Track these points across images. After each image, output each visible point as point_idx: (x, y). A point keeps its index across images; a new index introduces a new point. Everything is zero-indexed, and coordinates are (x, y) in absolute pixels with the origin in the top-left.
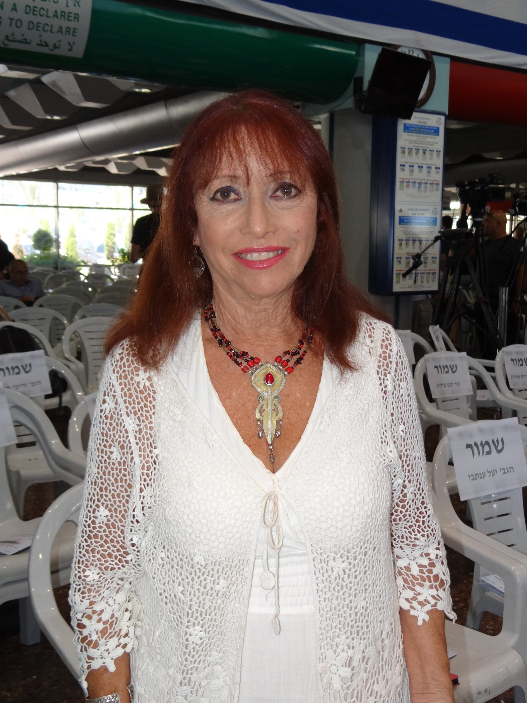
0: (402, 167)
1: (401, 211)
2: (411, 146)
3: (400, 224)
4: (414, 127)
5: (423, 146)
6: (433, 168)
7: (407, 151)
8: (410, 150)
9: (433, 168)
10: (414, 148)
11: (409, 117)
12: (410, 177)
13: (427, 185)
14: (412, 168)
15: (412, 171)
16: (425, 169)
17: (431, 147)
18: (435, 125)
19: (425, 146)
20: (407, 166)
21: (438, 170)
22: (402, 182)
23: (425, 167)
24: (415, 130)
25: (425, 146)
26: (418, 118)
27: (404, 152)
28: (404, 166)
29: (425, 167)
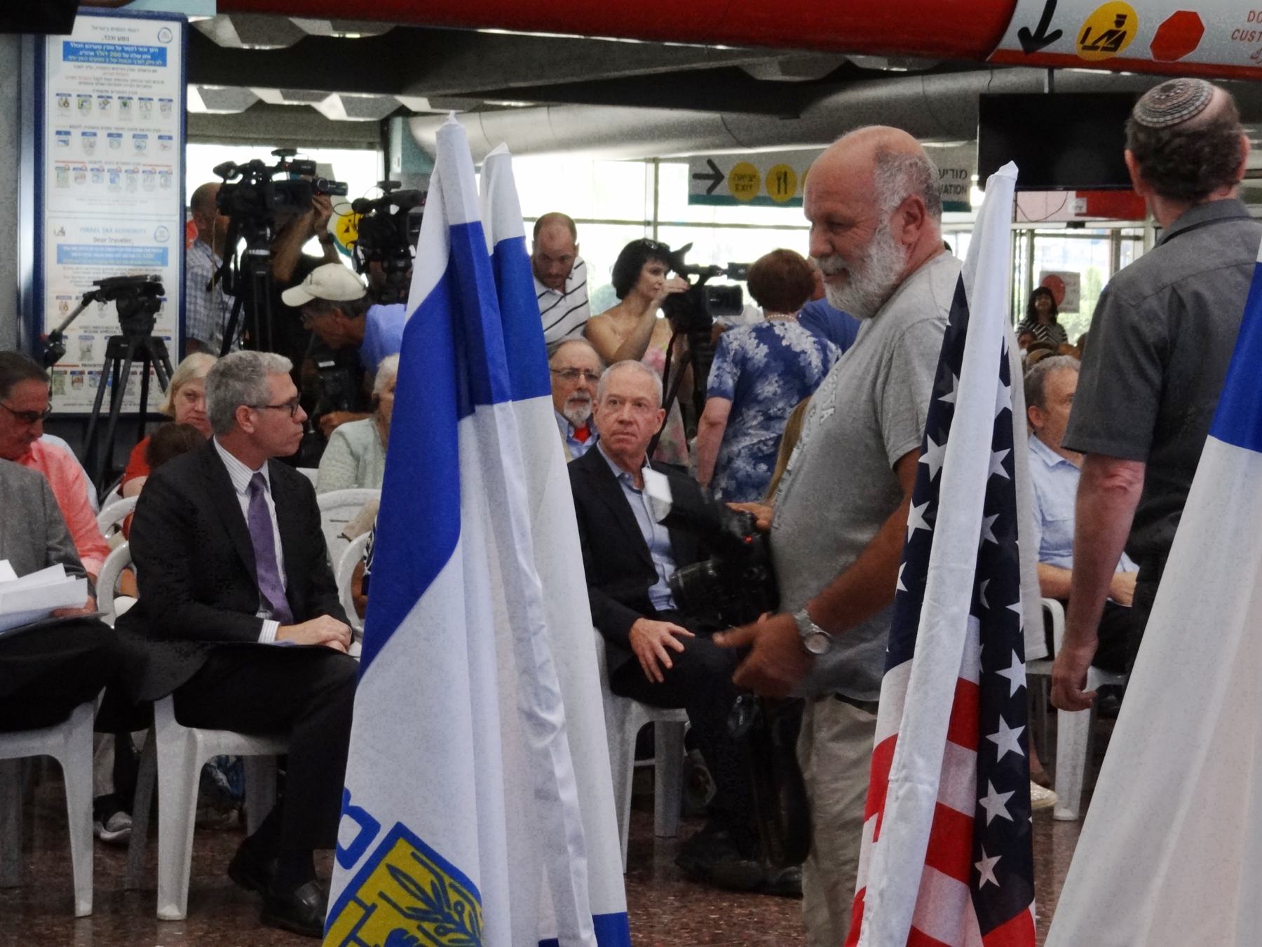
0: (64, 137)
1: (63, 232)
2: (87, 90)
3: (59, 261)
4: (92, 50)
5: (121, 89)
6: (153, 137)
7: (74, 101)
8: (84, 101)
9: (153, 137)
10: (95, 95)
11: (67, 29)
13: (134, 176)
14: (92, 139)
15: (92, 146)
17: (145, 93)
18: (155, 43)
19: (127, 89)
21: (166, 142)
22: (62, 170)
24: (95, 56)
25: (127, 89)
26: (102, 29)
27: (66, 104)
28: (68, 133)
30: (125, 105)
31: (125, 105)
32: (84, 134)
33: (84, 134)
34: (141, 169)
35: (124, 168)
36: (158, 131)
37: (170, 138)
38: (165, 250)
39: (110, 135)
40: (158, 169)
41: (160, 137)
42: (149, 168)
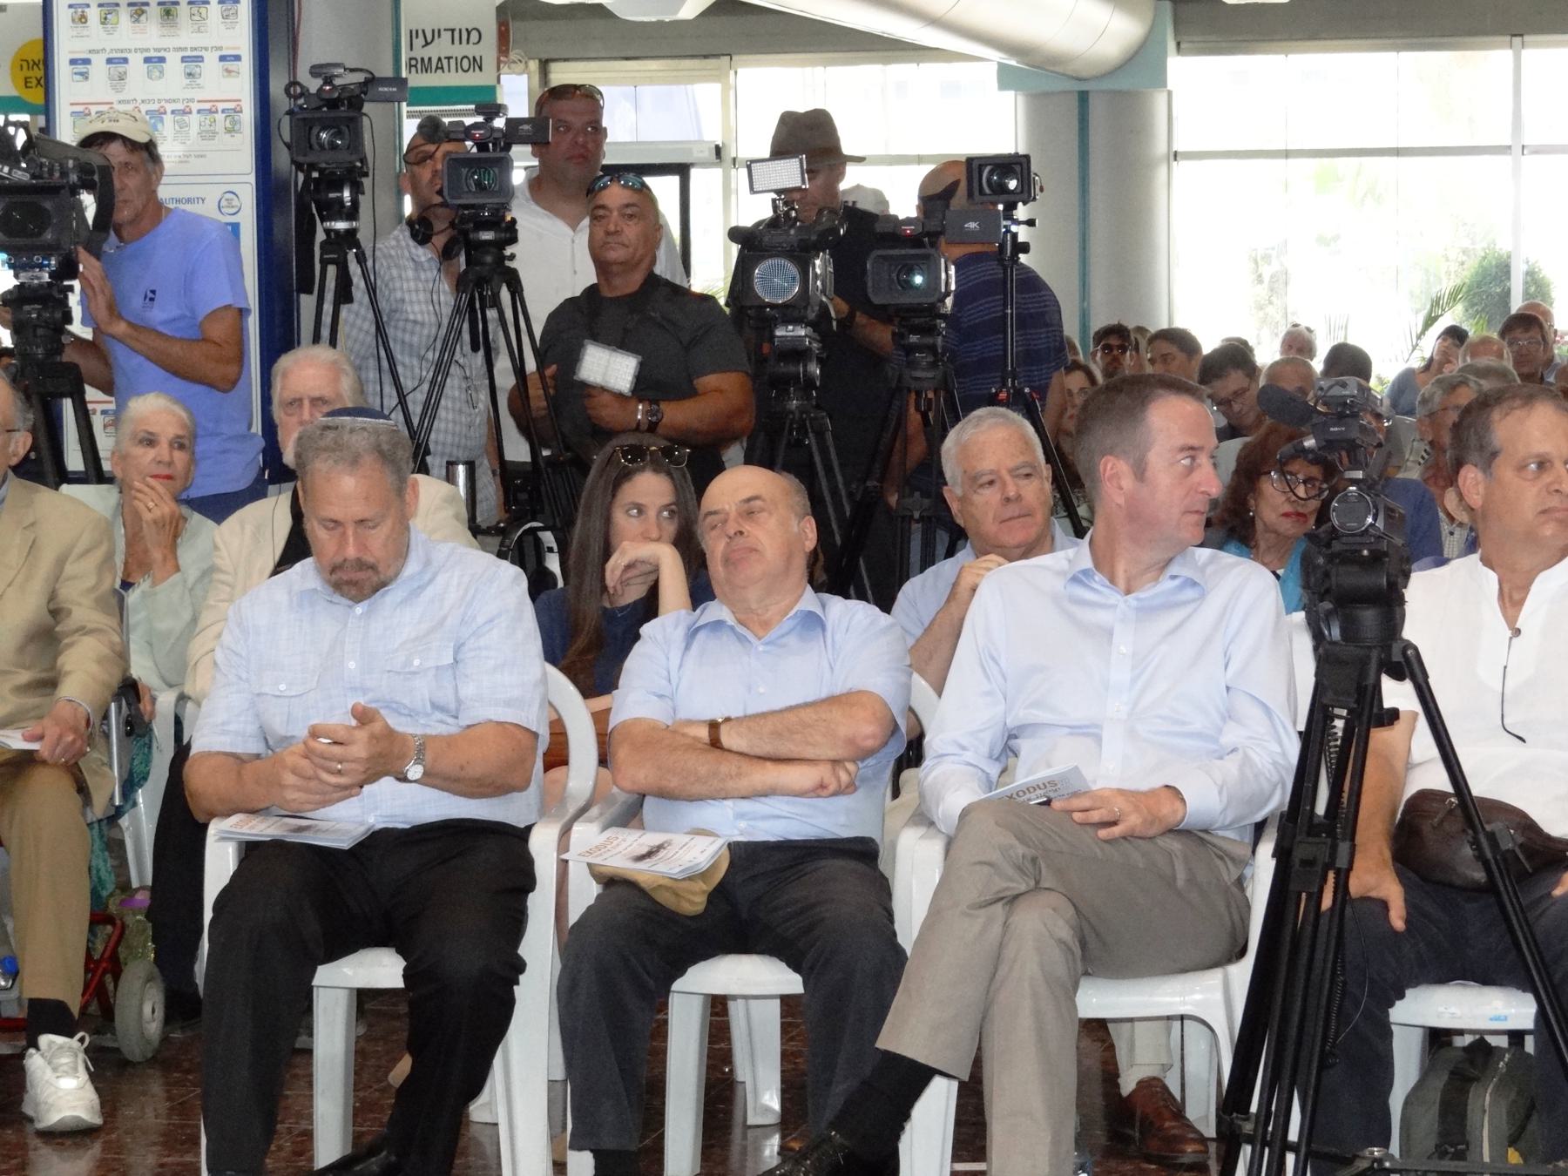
0: (81, 68)
6: (211, 58)
9: (211, 58)
12: (112, 97)
14: (121, 68)
15: (122, 77)
16: (174, 64)
20: (99, 62)
23: (173, 60)
27: (83, 19)
28: (87, 62)
29: (173, 60)
30: (168, 13)
31: (168, 13)
32: (109, 61)
33: (109, 61)
34: (195, 107)
35: (169, 107)
36: (220, 48)
37: (237, 58)
38: (235, 227)
39: (147, 60)
40: (221, 106)
41: (223, 58)
42: (207, 106)
